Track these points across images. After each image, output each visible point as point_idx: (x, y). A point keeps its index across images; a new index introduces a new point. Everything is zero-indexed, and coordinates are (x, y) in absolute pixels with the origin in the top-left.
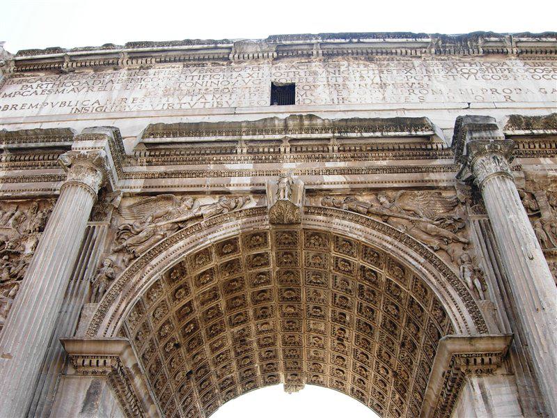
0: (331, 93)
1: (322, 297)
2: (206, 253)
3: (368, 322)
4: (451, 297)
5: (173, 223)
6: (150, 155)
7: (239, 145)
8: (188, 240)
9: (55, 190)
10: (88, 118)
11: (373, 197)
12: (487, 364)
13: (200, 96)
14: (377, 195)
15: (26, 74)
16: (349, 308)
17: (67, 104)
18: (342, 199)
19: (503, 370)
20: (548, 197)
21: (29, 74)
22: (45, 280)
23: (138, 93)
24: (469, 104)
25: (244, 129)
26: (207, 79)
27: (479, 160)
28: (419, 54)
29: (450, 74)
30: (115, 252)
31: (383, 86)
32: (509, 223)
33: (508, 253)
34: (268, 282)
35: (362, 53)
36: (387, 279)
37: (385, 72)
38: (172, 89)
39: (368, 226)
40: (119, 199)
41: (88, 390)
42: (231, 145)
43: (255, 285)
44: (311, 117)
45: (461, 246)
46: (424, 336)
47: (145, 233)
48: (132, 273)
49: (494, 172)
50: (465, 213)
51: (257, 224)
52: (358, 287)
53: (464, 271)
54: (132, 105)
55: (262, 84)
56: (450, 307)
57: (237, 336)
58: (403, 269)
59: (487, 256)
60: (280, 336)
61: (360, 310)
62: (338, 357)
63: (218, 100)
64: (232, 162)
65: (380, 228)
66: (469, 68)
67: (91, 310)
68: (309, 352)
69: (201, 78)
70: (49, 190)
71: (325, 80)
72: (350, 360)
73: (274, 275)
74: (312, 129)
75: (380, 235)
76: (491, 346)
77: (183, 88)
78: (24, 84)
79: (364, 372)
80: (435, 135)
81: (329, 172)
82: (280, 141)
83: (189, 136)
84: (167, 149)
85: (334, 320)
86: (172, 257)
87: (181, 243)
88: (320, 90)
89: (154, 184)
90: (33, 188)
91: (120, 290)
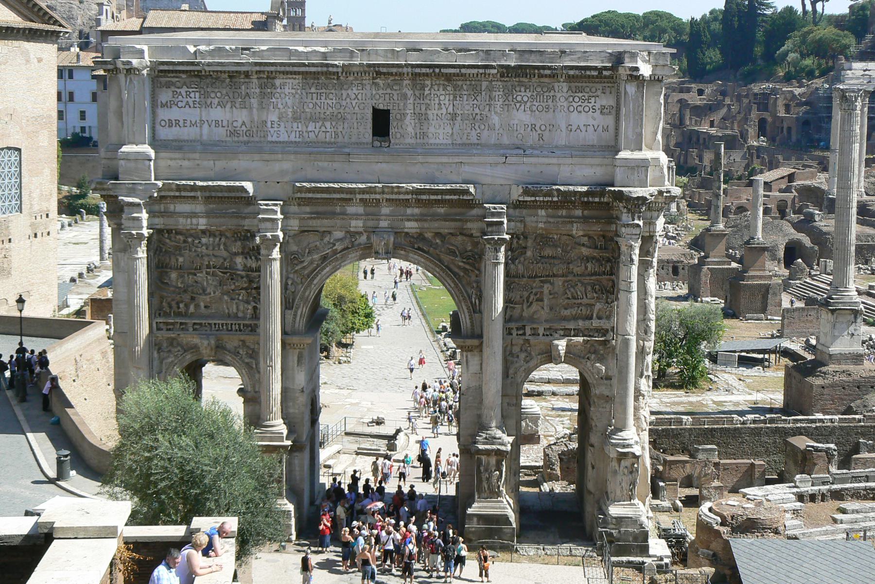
0: (415, 126)
13: (321, 123)
15: (169, 75)
21: (172, 75)
23: (273, 117)
24: (506, 157)
26: (323, 98)
29: (507, 102)
54: (272, 130)
55: (366, 111)
66: (523, 94)
67: (290, 314)
71: (411, 107)
74: (399, 193)
77: (307, 110)
78: (173, 88)
81: (409, 220)
87: (327, 269)
88: (408, 117)
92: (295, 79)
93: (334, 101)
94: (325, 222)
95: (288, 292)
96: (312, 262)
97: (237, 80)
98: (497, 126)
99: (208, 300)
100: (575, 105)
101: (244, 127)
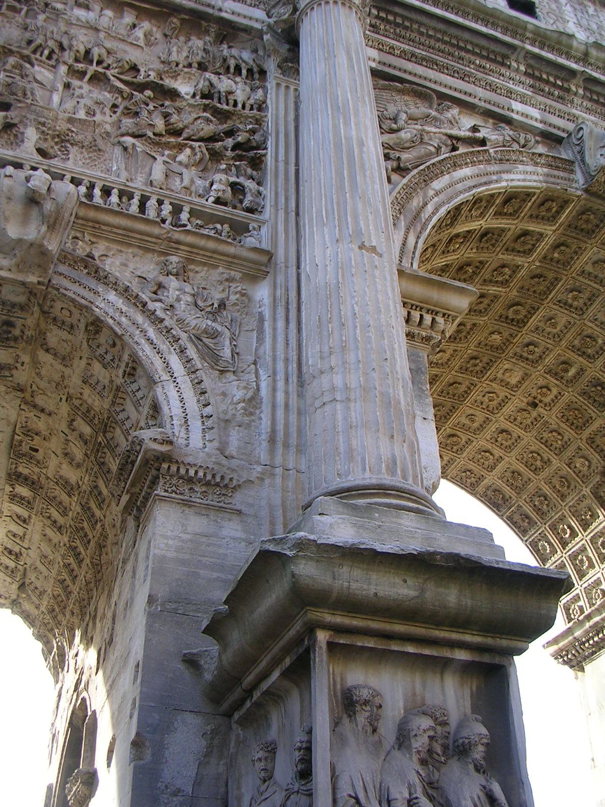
5: (446, 135)
6: (377, 17)
16: (589, 356)
42: (504, 50)
82: (573, 73)
86: (460, 186)
87: (466, 171)
96: (420, 139)
99: (62, 126)
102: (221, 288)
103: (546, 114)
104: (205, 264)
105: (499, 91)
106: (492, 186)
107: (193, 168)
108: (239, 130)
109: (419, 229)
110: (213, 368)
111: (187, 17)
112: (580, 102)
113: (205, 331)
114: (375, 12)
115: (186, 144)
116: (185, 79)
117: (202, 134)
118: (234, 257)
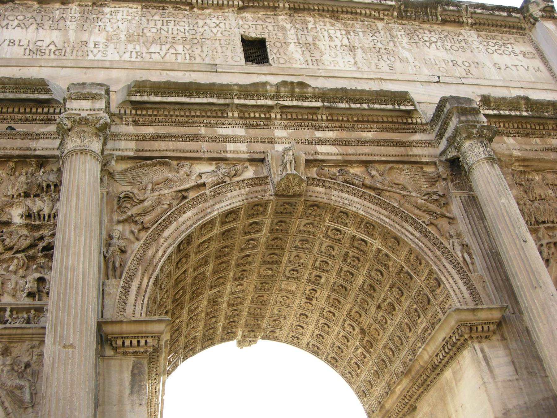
1: (302, 261)
2: (212, 222)
3: (345, 284)
4: (447, 270)
5: (177, 191)
6: (136, 115)
7: (230, 109)
8: (195, 210)
9: (35, 150)
10: (54, 65)
11: (363, 169)
12: (486, 332)
13: (168, 46)
14: (366, 167)
16: (327, 271)
17: (17, 42)
18: (334, 170)
19: (497, 337)
20: (513, 175)
22: (83, 262)
24: (439, 77)
25: (236, 93)
26: (171, 25)
27: (467, 143)
28: (381, 16)
29: (413, 40)
30: (119, 222)
31: (352, 49)
32: (502, 207)
33: (503, 235)
34: (254, 247)
35: (328, 11)
36: (378, 249)
37: (352, 33)
38: (136, 34)
39: (365, 199)
40: (113, 163)
41: (132, 371)
43: (242, 250)
44: (302, 85)
45: (447, 220)
46: (408, 302)
47: (150, 202)
48: (147, 246)
49: (483, 156)
50: (447, 188)
51: (260, 194)
52: (344, 253)
53: (453, 245)
56: (447, 279)
57: (211, 297)
58: (397, 240)
59: (471, 231)
60: (250, 296)
61: (339, 274)
62: (301, 314)
63: (190, 52)
64: (223, 126)
65: (376, 201)
66: (429, 36)
68: (272, 310)
69: (165, 24)
70: (28, 149)
71: (294, 37)
72: (314, 317)
73: (263, 240)
74: (303, 97)
75: (377, 208)
76: (490, 316)
77: (148, 34)
79: (327, 329)
80: (416, 110)
81: (321, 142)
82: (271, 107)
83: (178, 96)
84: (155, 108)
85: (309, 281)
86: (184, 227)
87: (189, 214)
88: (292, 48)
89: (147, 148)
90: (8, 146)
91: (139, 264)
92: (131, 8)
93: (187, 28)
94: (182, 145)
95: (111, 249)
97: (50, 6)
98: (411, 60)
100: (494, 49)
101: (53, 47)
102: (28, 354)
103: (252, 144)
104: (19, 342)
105: (218, 141)
106: (207, 218)
107: (21, 270)
108: (45, 237)
109: (151, 272)
110: (20, 407)
111: (17, 160)
112: (279, 123)
113: (16, 387)
114: (134, 112)
115: (14, 257)
116: (17, 205)
117: (23, 247)
118: (33, 334)
